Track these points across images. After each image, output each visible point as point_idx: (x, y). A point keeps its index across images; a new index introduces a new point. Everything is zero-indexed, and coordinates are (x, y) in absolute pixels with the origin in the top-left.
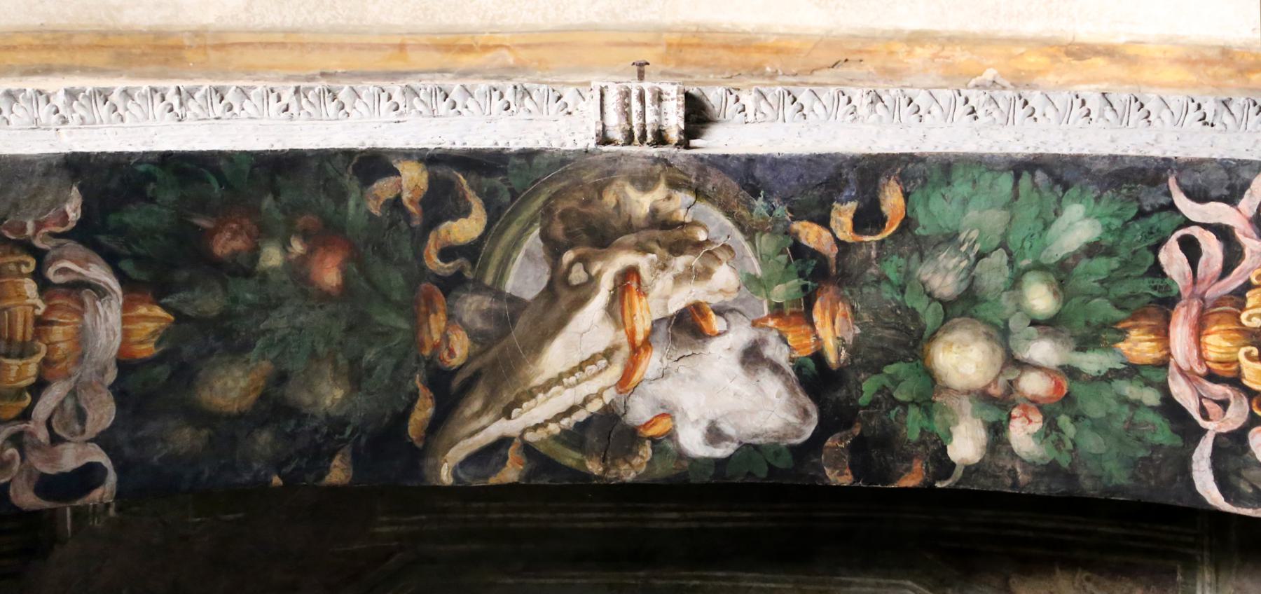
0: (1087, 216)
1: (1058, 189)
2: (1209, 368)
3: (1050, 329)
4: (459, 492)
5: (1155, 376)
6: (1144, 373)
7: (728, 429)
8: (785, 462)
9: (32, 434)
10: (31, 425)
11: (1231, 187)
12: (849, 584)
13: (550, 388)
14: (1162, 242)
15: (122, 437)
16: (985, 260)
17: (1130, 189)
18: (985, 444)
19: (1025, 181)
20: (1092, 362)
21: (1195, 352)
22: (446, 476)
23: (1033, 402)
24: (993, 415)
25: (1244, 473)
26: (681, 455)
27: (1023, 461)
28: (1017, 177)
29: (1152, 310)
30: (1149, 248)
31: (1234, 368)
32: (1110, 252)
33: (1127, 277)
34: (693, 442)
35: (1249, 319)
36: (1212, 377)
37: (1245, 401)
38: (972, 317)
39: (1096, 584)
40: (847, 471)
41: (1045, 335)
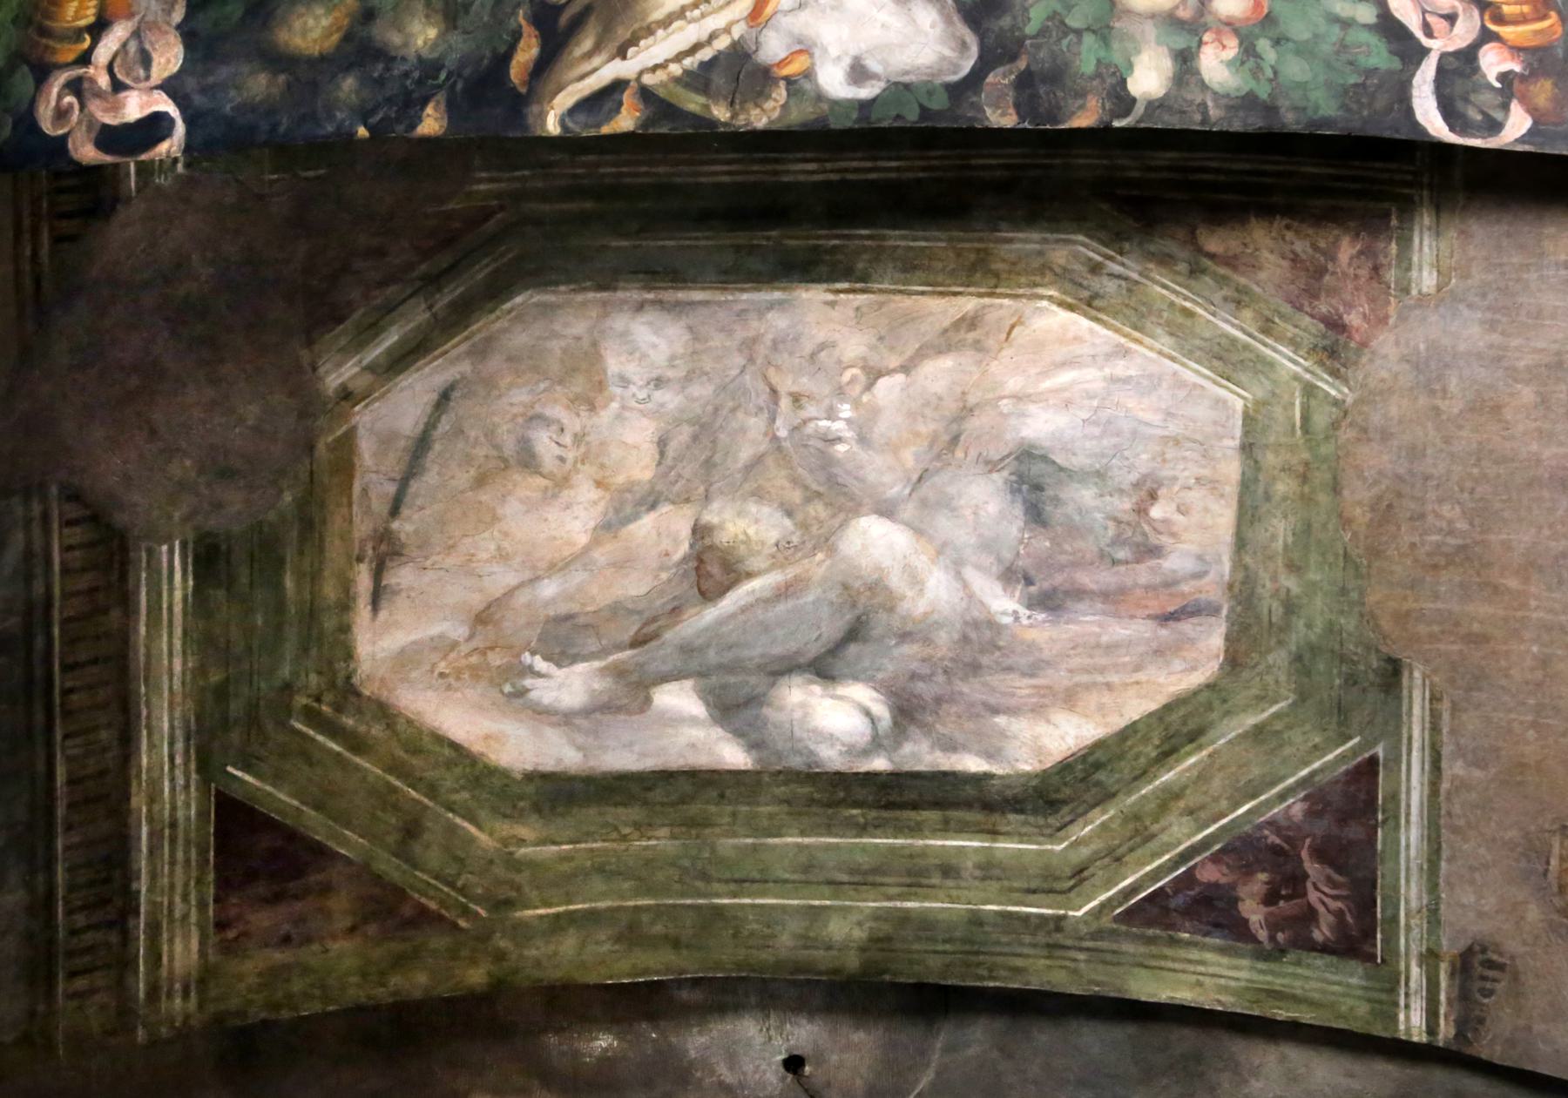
4: (567, 144)
7: (873, 65)
8: (939, 103)
9: (92, 81)
10: (91, 70)
12: (1010, 241)
13: (670, 24)
15: (191, 83)
18: (1171, 75)
22: (552, 126)
23: (1228, 24)
24: (1181, 42)
25: (1473, 97)
26: (820, 97)
27: (1215, 93)
34: (834, 82)
37: (1476, 13)
40: (1011, 110)
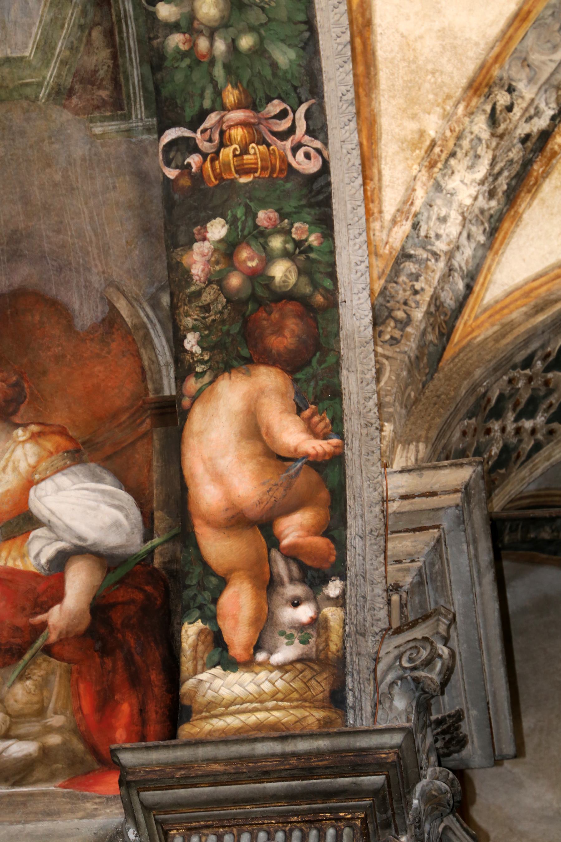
0: (290, 61)
1: (302, 45)
2: (226, 131)
3: (232, 49)
5: (217, 106)
6: (218, 99)
11: (314, 131)
14: (283, 100)
16: (261, 12)
17: (306, 81)
18: (169, 21)
19: (303, 27)
20: (219, 72)
21: (232, 123)
24: (183, 24)
25: (179, 153)
27: (164, 42)
28: (305, 23)
29: (250, 100)
30: (279, 95)
31: (228, 143)
32: (274, 75)
33: (263, 84)
35: (253, 148)
36: (222, 133)
37: (213, 150)
38: (232, 8)
39: (107, 71)
41: (228, 46)
